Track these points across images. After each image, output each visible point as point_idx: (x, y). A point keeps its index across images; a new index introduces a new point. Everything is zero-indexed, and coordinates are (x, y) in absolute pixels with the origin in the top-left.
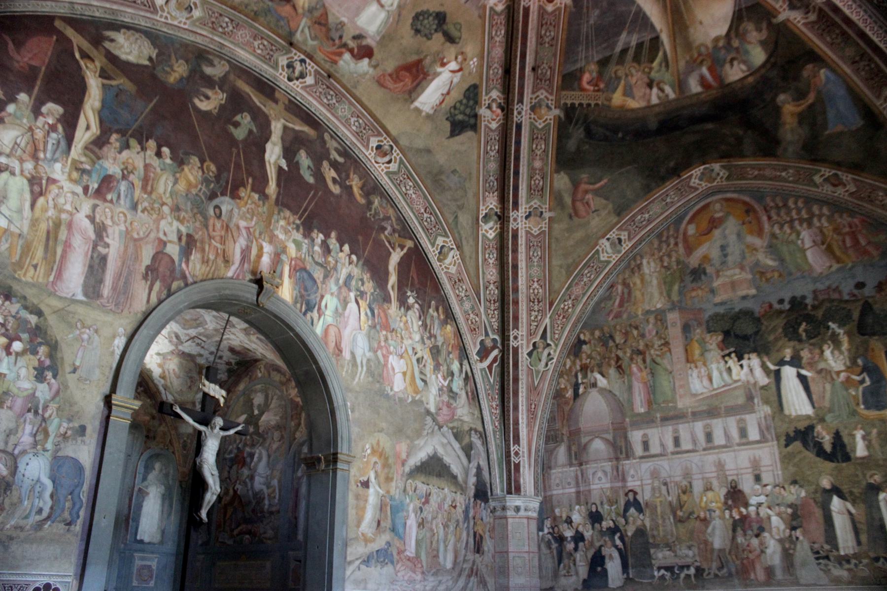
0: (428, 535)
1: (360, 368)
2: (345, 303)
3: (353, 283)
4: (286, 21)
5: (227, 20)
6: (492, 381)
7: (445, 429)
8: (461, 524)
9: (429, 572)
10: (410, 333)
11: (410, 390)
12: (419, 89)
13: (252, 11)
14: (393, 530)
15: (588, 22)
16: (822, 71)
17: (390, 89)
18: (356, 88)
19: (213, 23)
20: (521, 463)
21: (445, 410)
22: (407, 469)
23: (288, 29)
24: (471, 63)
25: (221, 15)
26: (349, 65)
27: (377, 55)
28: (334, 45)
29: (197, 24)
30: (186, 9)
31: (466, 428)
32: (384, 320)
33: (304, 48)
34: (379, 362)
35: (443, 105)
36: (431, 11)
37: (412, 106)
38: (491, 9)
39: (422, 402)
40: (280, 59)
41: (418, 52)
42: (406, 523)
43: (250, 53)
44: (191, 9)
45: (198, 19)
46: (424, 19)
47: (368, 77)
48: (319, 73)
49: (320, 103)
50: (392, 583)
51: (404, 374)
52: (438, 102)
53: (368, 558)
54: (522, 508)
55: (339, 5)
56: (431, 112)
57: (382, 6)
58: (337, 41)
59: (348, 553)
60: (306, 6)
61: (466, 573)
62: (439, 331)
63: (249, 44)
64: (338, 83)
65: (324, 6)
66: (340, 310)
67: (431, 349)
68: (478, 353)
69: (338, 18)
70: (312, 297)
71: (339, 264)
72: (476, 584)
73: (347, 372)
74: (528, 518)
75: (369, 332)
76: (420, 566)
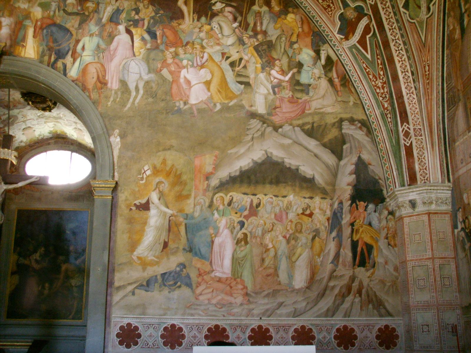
0: (256, 251)
1: (134, 94)
2: (111, 37)
3: (123, 16)
6: (369, 56)
7: (287, 128)
8: (323, 234)
9: (256, 293)
10: (218, 39)
11: (217, 98)
14: (191, 249)
20: (414, 144)
21: (286, 107)
22: (214, 182)
31: (330, 120)
32: (171, 37)
34: (164, 80)
39: (242, 107)
42: (213, 242)
50: (188, 307)
51: (208, 84)
53: (148, 283)
54: (419, 202)
59: (116, 278)
61: (336, 291)
62: (271, 26)
66: (103, 46)
67: (256, 48)
68: (340, 32)
70: (64, 46)
71: (101, 5)
72: (357, 306)
73: (114, 101)
74: (429, 214)
75: (148, 55)
76: (240, 287)
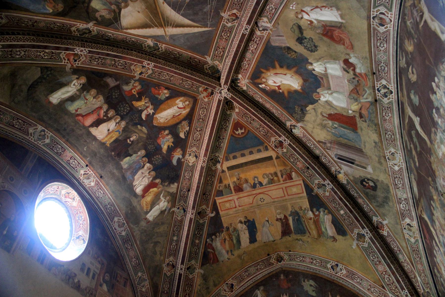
4: (369, 110)
5: (387, 136)
12: (333, 24)
13: (376, 127)
15: (212, 6)
16: (51, 11)
17: (349, 40)
18: (366, 57)
19: (392, 141)
23: (371, 106)
24: (294, 8)
25: (387, 140)
26: (360, 68)
27: (344, 57)
28: (360, 80)
29: (397, 148)
30: (393, 155)
33: (373, 93)
35: (324, 5)
36: (303, 47)
37: (343, 21)
38: (270, 23)
40: (386, 103)
41: (321, 39)
43: (394, 118)
44: (392, 153)
45: (395, 149)
46: (309, 48)
47: (356, 55)
48: (377, 79)
49: (390, 71)
52: (327, 8)
55: (344, 87)
56: (334, 8)
57: (326, 68)
58: (357, 79)
60: (356, 103)
63: (390, 122)
64: (373, 67)
65: (350, 95)
69: (349, 85)
